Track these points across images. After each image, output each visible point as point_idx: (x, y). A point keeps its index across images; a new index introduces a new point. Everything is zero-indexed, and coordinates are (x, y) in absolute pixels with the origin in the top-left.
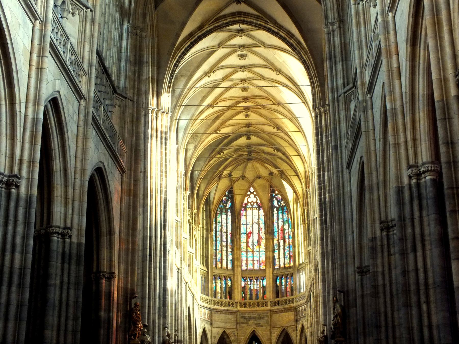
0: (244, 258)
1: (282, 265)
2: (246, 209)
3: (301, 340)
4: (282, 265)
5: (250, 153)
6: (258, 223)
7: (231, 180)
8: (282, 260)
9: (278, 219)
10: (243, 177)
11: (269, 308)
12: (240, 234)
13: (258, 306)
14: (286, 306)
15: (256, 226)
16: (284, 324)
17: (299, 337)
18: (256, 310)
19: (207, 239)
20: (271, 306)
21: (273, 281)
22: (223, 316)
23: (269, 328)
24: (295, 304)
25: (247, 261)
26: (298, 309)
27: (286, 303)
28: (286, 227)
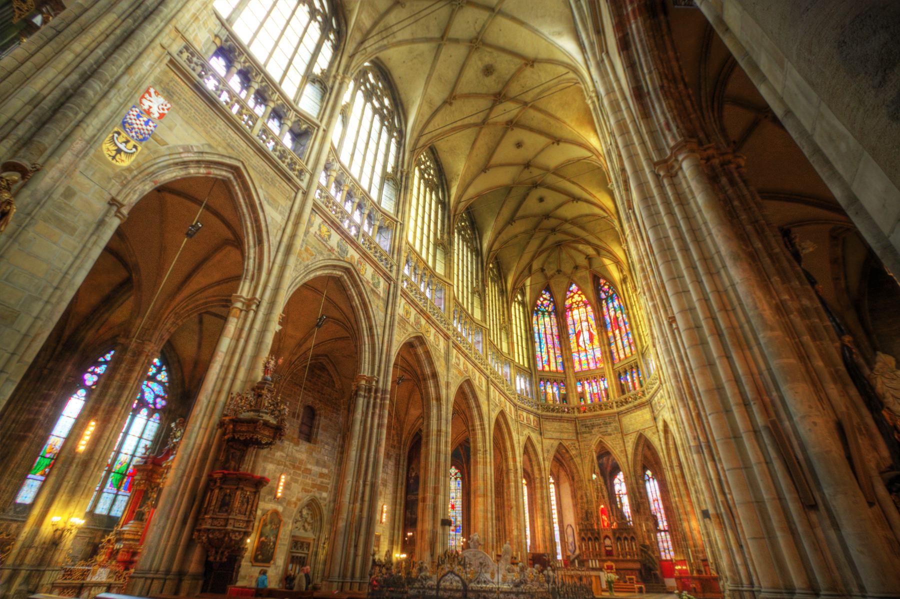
0: (577, 359)
1: (622, 356)
2: (571, 308)
3: (667, 444)
4: (622, 356)
5: (553, 230)
6: (587, 320)
7: (546, 277)
8: (621, 352)
9: (608, 310)
10: (559, 271)
11: (615, 410)
12: (568, 335)
13: (601, 409)
14: (636, 403)
15: (585, 324)
16: (639, 427)
17: (663, 440)
18: (598, 415)
19: (527, 339)
20: (617, 406)
21: (615, 378)
22: (556, 425)
23: (620, 436)
24: (648, 397)
25: (580, 361)
26: (653, 402)
27: (636, 399)
28: (619, 314)
